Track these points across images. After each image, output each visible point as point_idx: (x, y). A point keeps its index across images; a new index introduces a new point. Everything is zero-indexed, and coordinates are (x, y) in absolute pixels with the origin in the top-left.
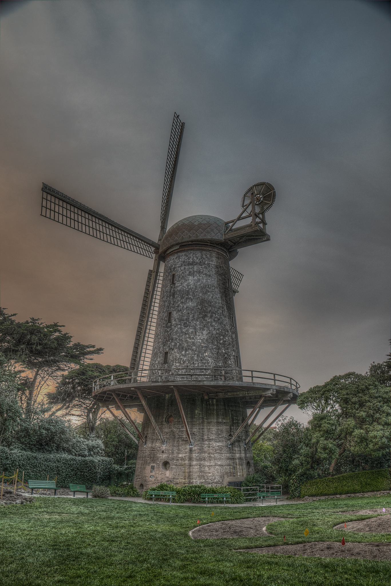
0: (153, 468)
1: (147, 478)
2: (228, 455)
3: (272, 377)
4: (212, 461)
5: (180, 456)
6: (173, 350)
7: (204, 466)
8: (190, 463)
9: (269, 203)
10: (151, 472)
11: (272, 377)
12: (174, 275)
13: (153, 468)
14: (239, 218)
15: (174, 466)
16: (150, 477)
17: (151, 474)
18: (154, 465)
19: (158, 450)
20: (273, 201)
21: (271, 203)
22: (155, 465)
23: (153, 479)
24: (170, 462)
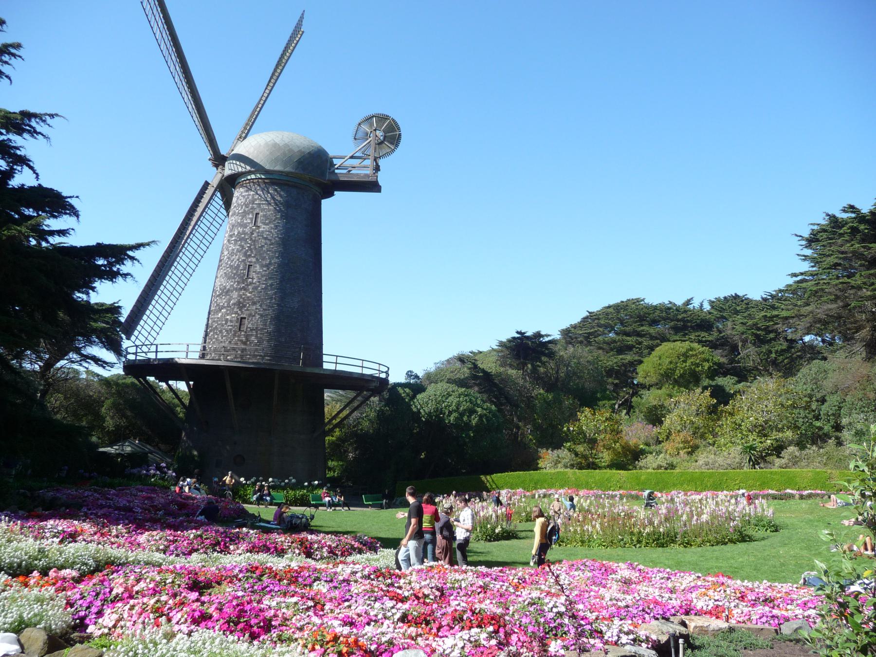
3: (359, 363)
11: (359, 363)
12: (257, 214)
14: (352, 157)
20: (397, 146)
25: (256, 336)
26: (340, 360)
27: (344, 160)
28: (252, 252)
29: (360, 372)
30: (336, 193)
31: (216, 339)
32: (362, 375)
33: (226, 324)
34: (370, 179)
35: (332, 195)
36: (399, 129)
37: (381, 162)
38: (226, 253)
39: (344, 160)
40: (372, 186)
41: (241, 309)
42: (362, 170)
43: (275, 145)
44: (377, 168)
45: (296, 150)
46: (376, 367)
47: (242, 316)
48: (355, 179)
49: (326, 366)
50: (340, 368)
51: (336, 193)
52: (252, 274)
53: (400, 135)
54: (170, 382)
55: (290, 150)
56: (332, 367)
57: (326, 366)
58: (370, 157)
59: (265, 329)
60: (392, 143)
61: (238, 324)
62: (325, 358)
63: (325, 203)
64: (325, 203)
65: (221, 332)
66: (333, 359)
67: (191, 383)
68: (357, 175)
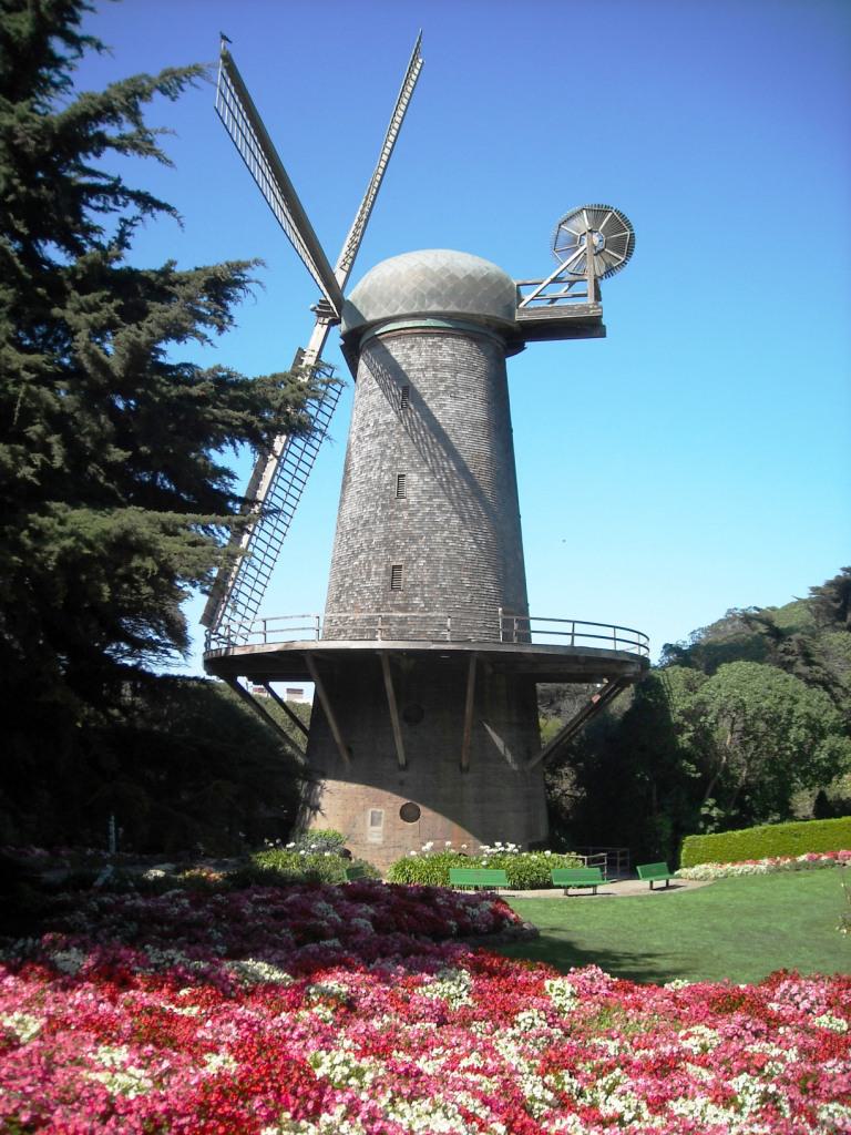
18: (379, 810)
20: (629, 254)
21: (623, 259)
22: (383, 811)
25: (423, 598)
26: (579, 629)
27: (541, 287)
28: (401, 451)
29: (612, 648)
30: (527, 344)
31: (354, 606)
32: (616, 652)
33: (368, 578)
34: (591, 313)
36: (630, 227)
37: (605, 285)
38: (355, 459)
39: (541, 287)
41: (391, 551)
42: (572, 304)
43: (425, 270)
44: (598, 297)
45: (461, 276)
46: (609, 632)
48: (565, 315)
49: (536, 639)
51: (527, 344)
52: (409, 492)
53: (632, 235)
55: (452, 277)
57: (536, 639)
59: (437, 583)
60: (621, 253)
61: (389, 578)
62: (534, 625)
63: (513, 364)
64: (510, 361)
65: (359, 593)
68: (572, 308)
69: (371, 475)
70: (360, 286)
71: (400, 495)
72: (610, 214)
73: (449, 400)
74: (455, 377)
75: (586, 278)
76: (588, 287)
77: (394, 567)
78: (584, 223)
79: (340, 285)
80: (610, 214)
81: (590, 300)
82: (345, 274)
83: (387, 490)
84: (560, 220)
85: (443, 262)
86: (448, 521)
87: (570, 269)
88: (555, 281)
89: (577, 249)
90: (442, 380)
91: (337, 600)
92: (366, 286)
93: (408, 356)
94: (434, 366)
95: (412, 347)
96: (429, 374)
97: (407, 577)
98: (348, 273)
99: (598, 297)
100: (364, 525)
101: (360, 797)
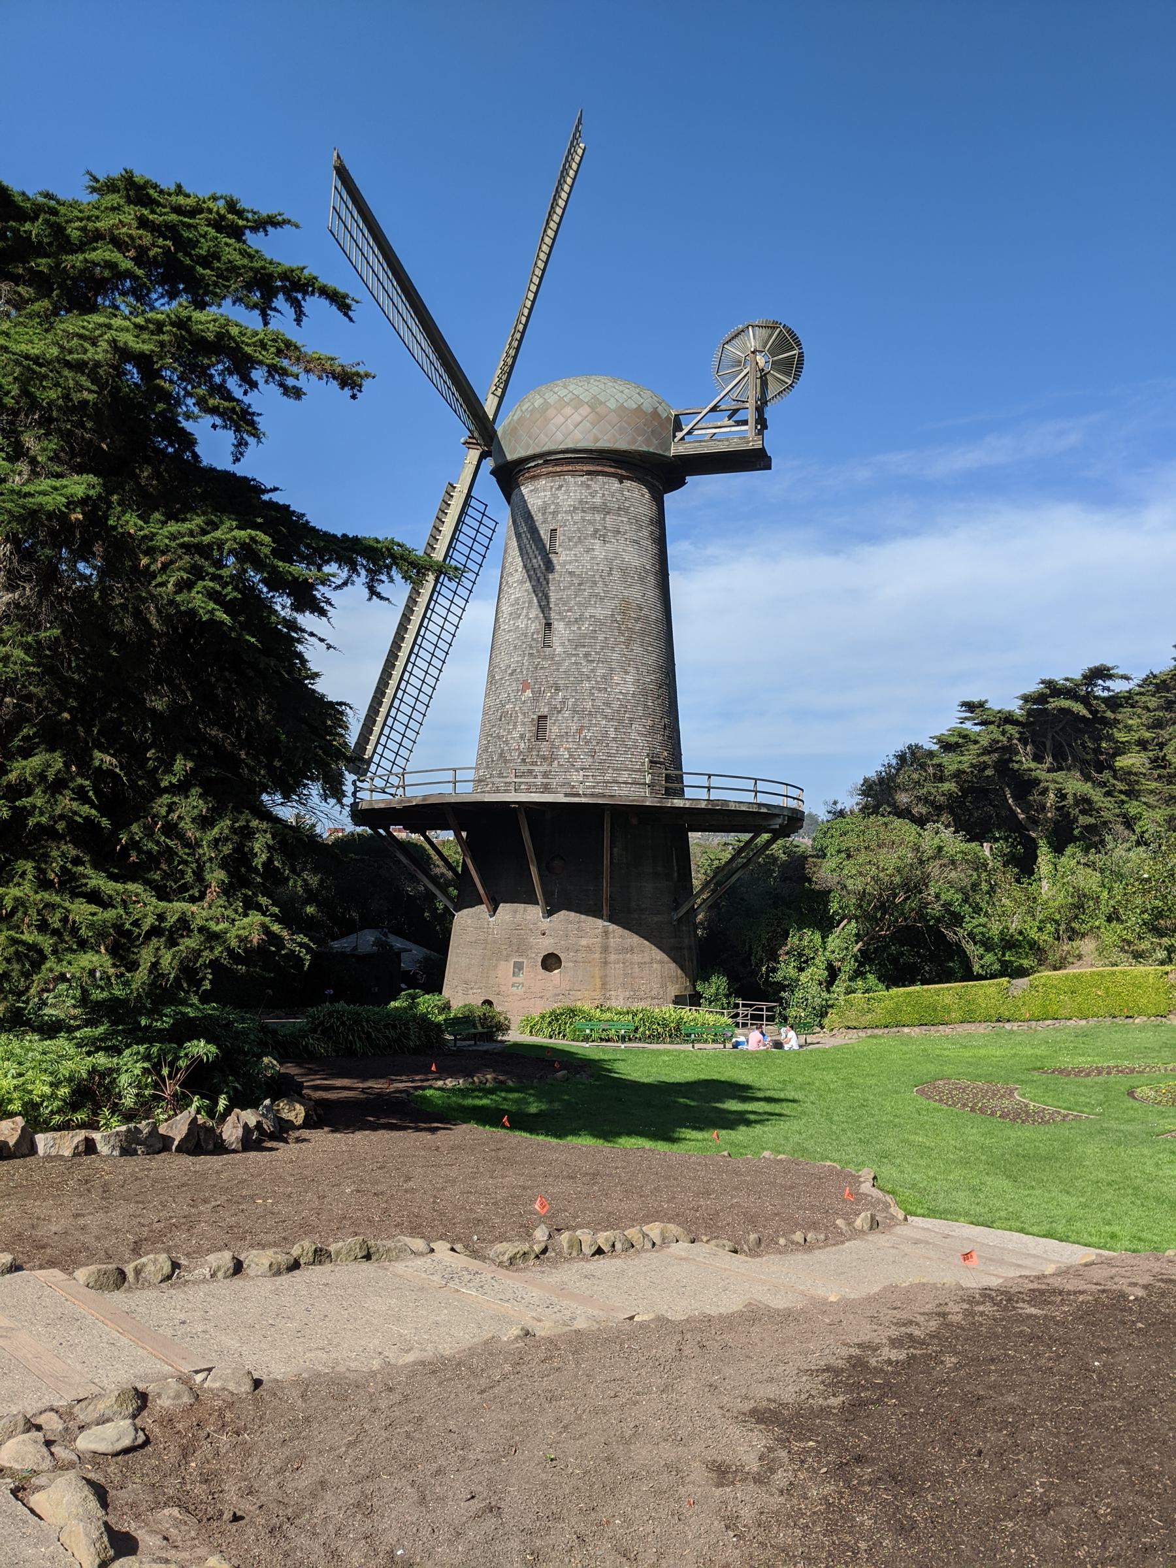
0: (518, 967)
1: (503, 988)
2: (672, 940)
3: (750, 785)
4: (646, 954)
5: (584, 942)
6: (559, 712)
7: (631, 963)
8: (605, 958)
9: (787, 380)
10: (514, 975)
11: (750, 785)
13: (518, 967)
15: (571, 964)
16: (513, 986)
17: (515, 979)
19: (531, 930)
20: (797, 377)
21: (790, 382)
23: (521, 991)
24: (562, 956)
26: (715, 781)
30: (688, 479)
35: (682, 483)
36: (799, 344)
40: (755, 460)
44: (762, 423)
47: (539, 714)
50: (715, 795)
51: (688, 479)
52: (556, 641)
53: (801, 355)
54: (431, 834)
56: (702, 794)
58: (747, 405)
60: (788, 374)
62: (687, 780)
66: (703, 781)
67: (464, 834)
69: (519, 623)
70: (506, 421)
71: (547, 645)
72: (779, 330)
73: (597, 544)
74: (604, 519)
75: (747, 405)
76: (751, 415)
77: (540, 717)
78: (752, 340)
79: (491, 417)
80: (779, 330)
81: (749, 430)
82: (496, 400)
83: (533, 639)
84: (727, 337)
85: (594, 390)
86: (593, 671)
87: (734, 395)
88: (714, 409)
89: (742, 370)
90: (591, 523)
91: (486, 750)
92: (515, 418)
93: (555, 496)
94: (581, 507)
95: (561, 487)
96: (578, 517)
97: (553, 730)
98: (501, 398)
99: (762, 423)
100: (511, 674)
101: (503, 947)
